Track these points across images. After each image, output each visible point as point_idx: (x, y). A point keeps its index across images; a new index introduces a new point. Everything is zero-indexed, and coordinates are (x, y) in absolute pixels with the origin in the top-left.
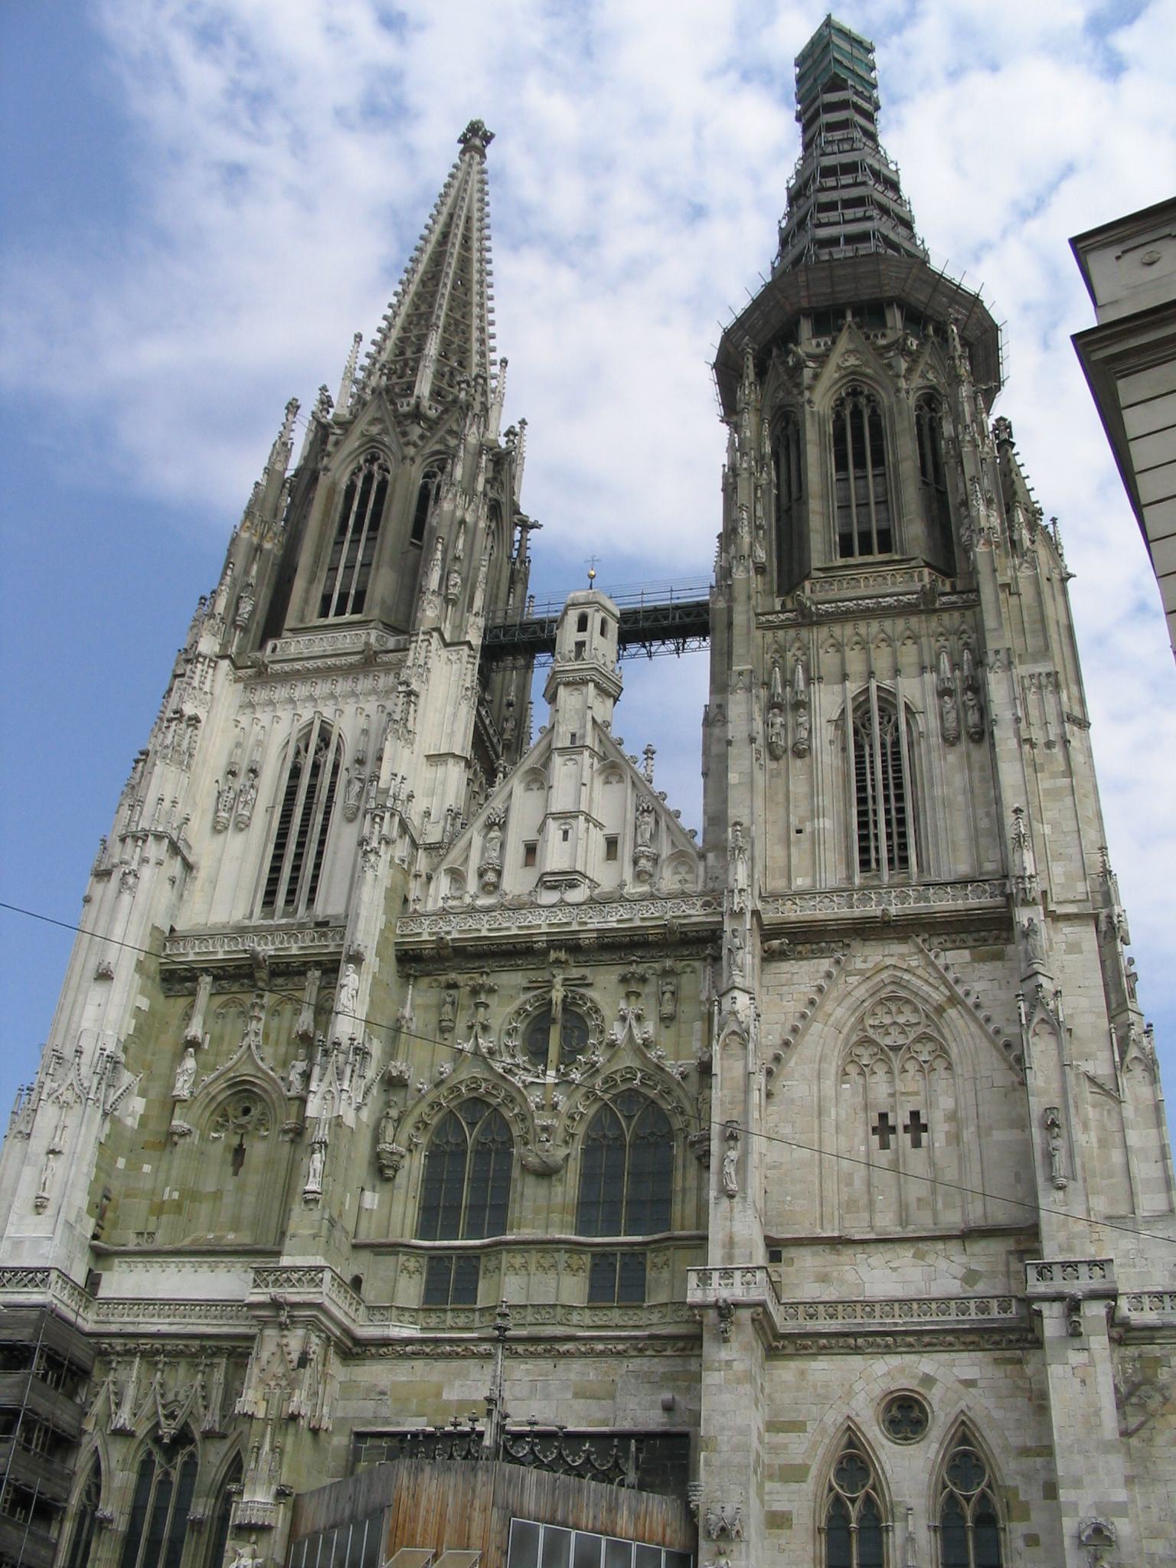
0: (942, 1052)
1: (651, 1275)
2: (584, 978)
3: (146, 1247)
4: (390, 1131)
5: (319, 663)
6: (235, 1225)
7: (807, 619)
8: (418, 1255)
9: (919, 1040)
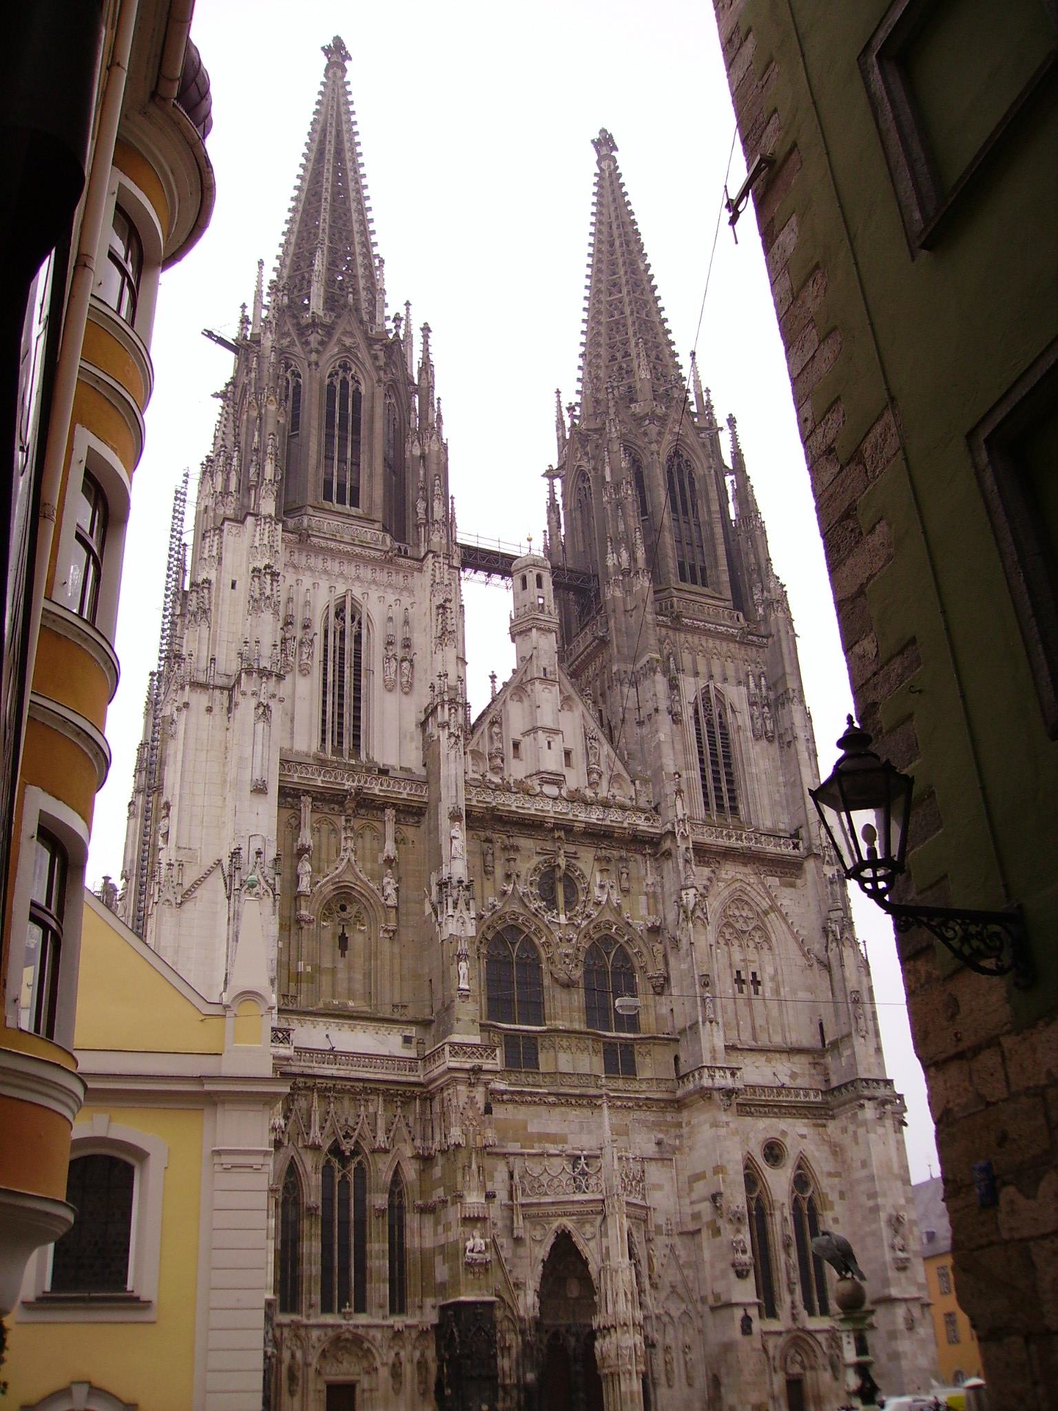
0: (767, 939)
1: (638, 1059)
2: (575, 853)
3: (290, 1007)
5: (349, 548)
6: (351, 994)
7: (677, 623)
8: (499, 1033)
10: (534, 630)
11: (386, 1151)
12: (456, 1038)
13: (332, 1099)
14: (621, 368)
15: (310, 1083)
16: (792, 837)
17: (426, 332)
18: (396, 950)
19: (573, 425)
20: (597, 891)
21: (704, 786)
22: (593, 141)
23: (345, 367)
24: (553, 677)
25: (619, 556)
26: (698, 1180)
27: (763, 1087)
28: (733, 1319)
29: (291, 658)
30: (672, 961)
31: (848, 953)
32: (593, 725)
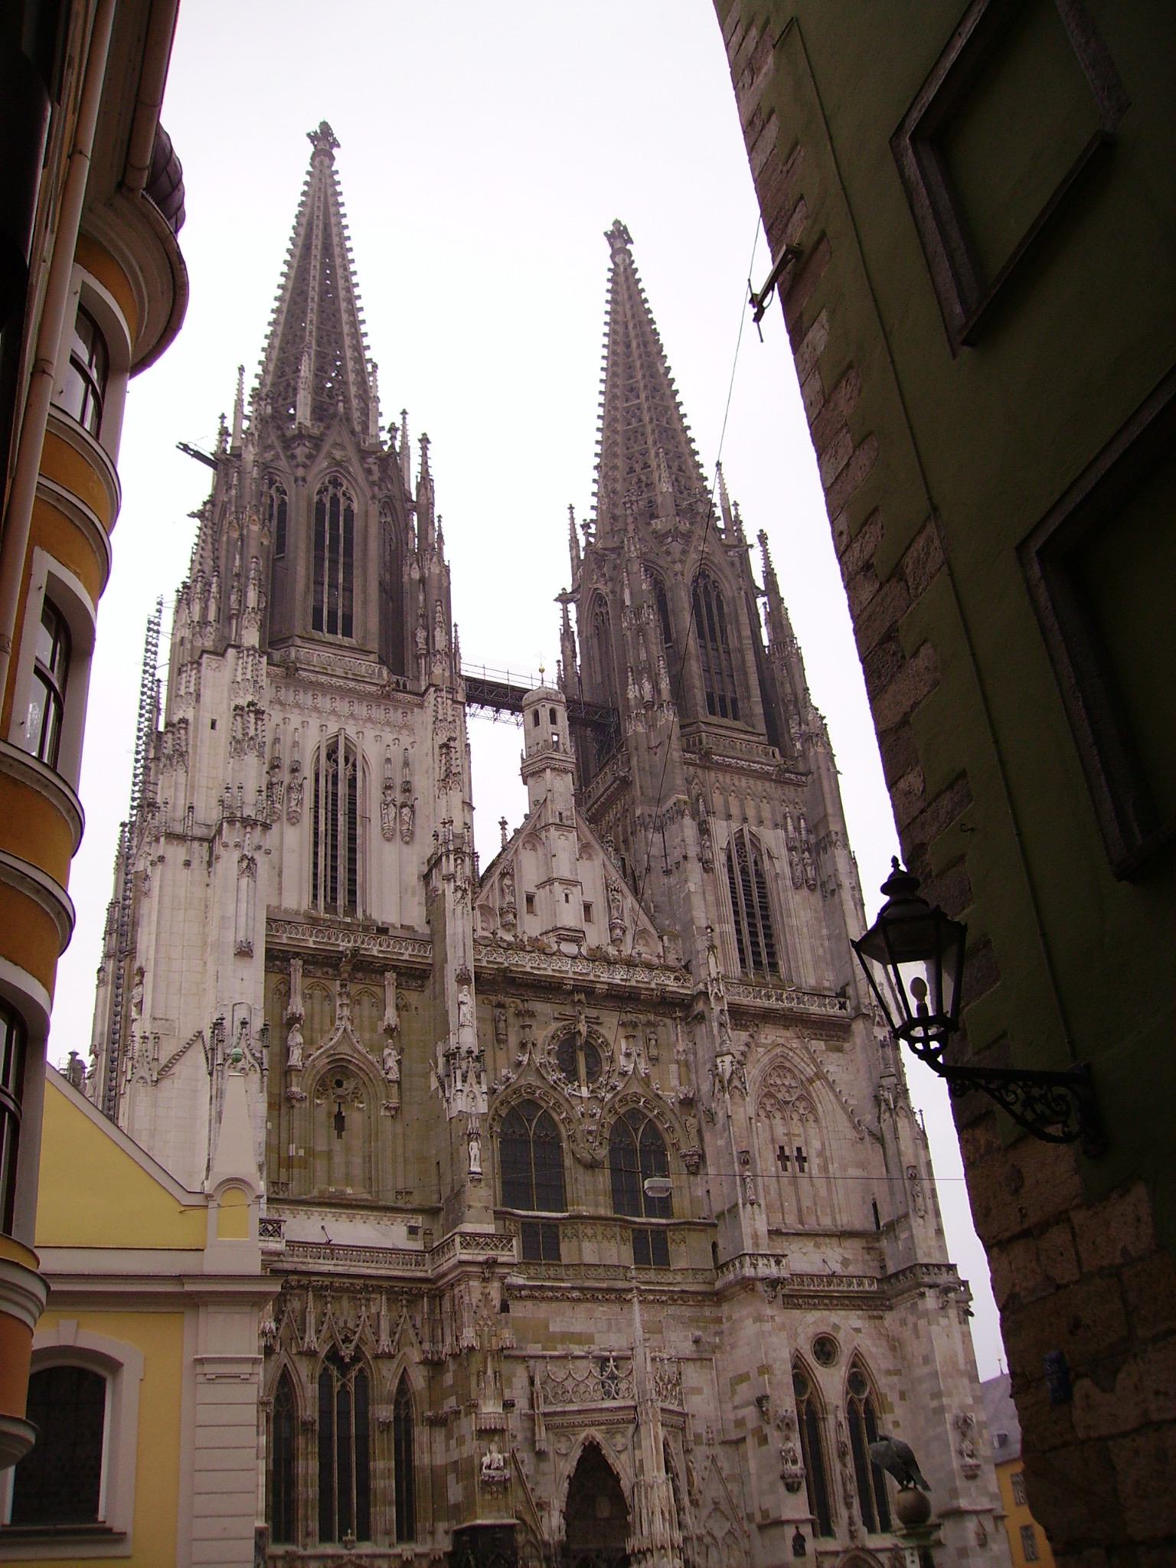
0: (813, 1109)
1: (671, 1247)
2: (598, 1018)
3: (281, 1196)
5: (341, 682)
6: (348, 1180)
7: (705, 760)
9: (797, 1099)
10: (548, 771)
11: (391, 1356)
12: (468, 1227)
13: (329, 1299)
14: (640, 481)
15: (304, 1281)
16: (838, 995)
17: (424, 443)
18: (399, 1130)
19: (588, 543)
20: (622, 1060)
21: (740, 941)
22: (606, 234)
23: (335, 483)
24: (569, 823)
25: (641, 688)
26: (742, 1382)
27: (812, 1276)
28: (783, 1538)
29: (277, 805)
30: (707, 1136)
31: (902, 1124)
32: (615, 876)
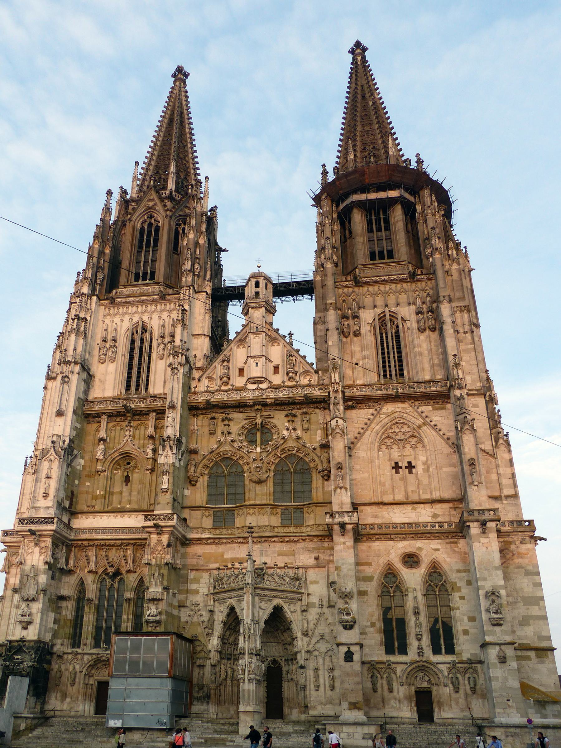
1: (306, 516)
4: (192, 470)
9: (410, 437)
20: (286, 433)
